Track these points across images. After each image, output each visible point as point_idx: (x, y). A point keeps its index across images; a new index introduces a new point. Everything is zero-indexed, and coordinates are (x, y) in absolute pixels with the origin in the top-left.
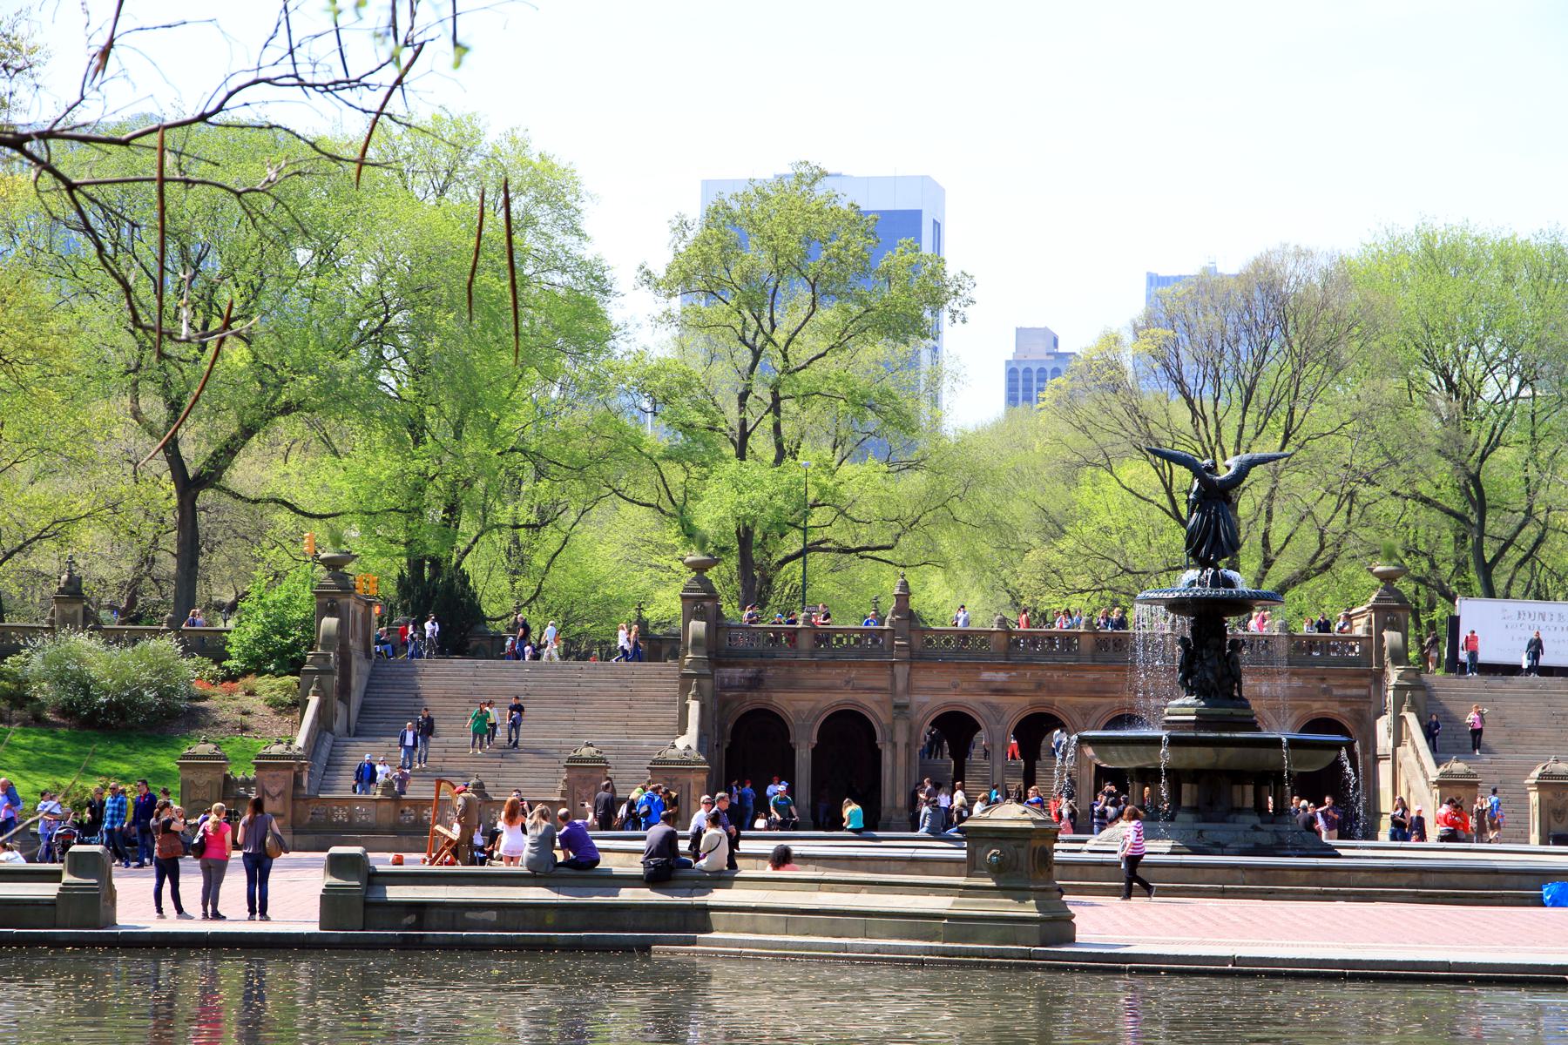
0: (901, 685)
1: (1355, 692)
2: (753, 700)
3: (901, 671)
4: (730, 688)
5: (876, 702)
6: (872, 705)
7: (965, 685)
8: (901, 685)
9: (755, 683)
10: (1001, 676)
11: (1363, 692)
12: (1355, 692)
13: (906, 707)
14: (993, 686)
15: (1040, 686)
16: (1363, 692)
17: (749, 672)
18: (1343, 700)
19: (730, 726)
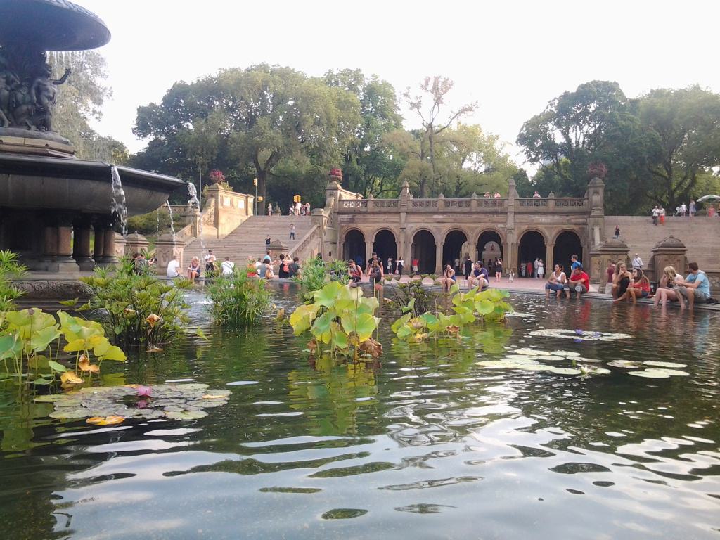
0: (403, 220)
1: (581, 221)
2: (352, 226)
3: (403, 215)
4: (344, 222)
5: (395, 227)
6: (394, 228)
7: (426, 221)
8: (403, 220)
9: (352, 220)
10: (440, 217)
11: (584, 220)
12: (581, 221)
13: (405, 228)
14: (437, 221)
15: (455, 221)
16: (584, 220)
17: (350, 216)
18: (576, 224)
19: (344, 236)
